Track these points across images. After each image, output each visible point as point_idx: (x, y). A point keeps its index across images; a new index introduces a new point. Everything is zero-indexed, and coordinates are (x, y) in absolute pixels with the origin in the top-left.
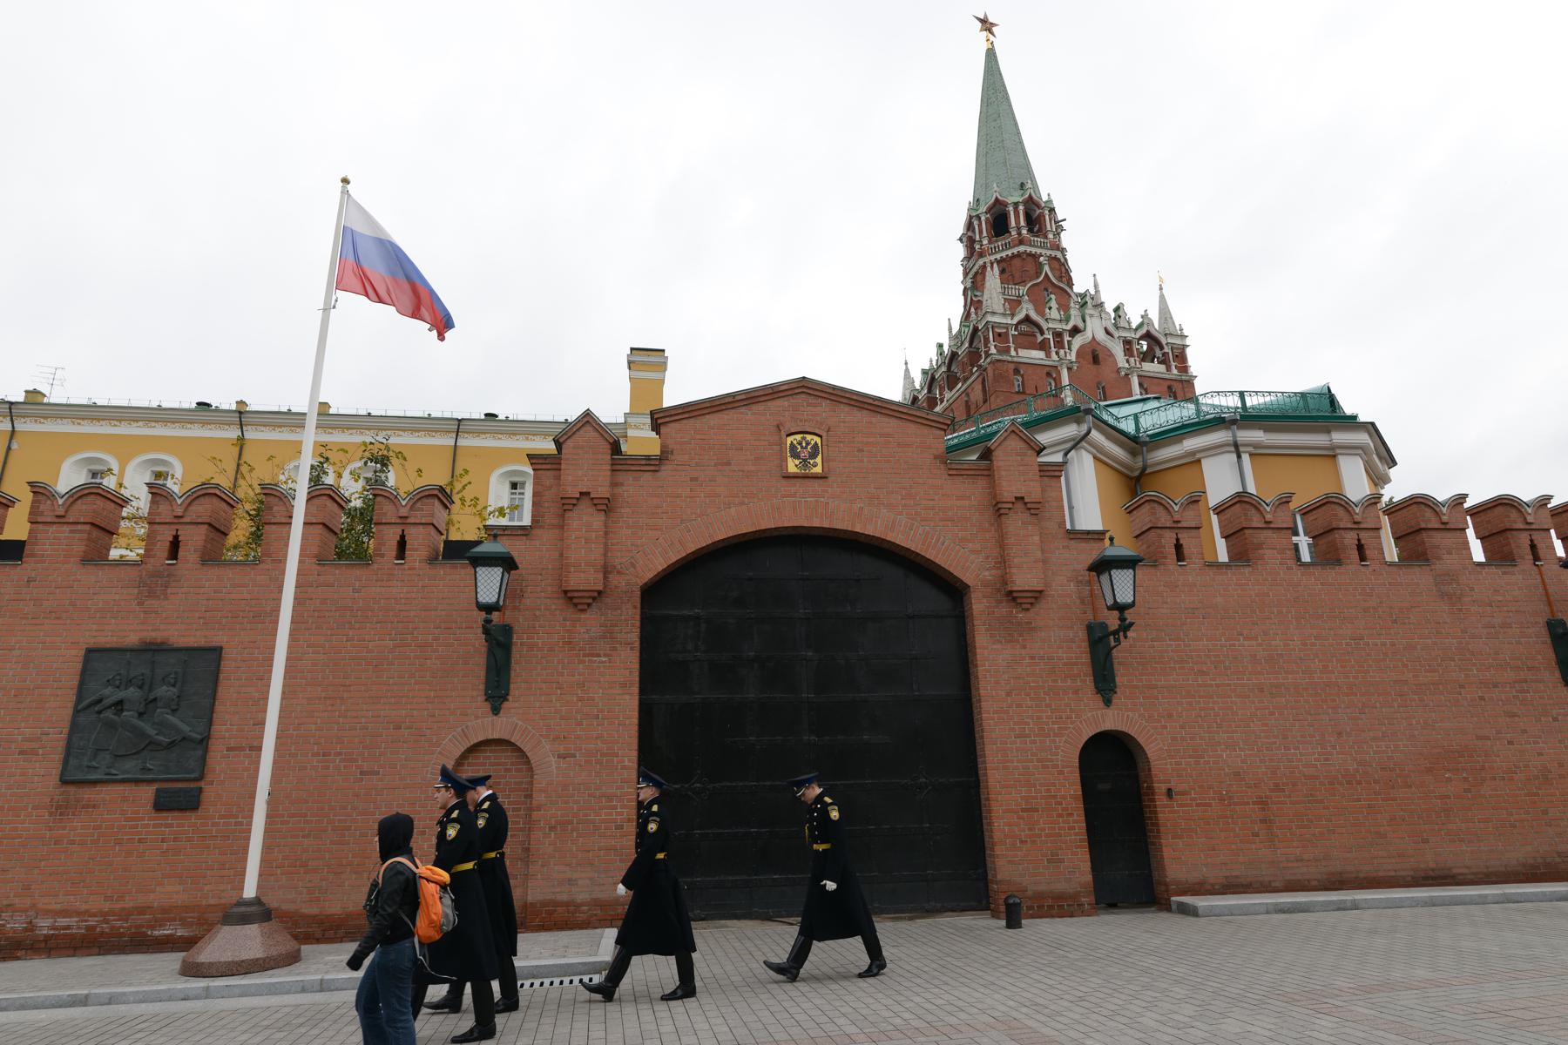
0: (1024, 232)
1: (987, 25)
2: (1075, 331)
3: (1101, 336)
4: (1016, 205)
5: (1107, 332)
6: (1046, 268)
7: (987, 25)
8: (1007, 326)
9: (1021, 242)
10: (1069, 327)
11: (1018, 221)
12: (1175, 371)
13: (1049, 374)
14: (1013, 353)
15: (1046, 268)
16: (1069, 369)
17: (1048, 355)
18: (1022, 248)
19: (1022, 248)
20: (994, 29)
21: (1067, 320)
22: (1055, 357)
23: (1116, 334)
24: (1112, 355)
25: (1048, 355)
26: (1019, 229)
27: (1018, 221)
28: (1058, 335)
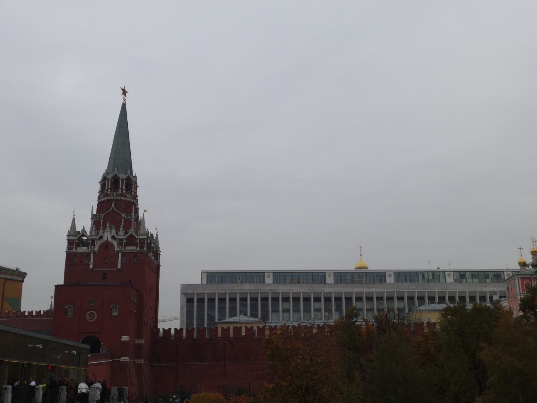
0: (109, 191)
1: (124, 92)
2: (101, 237)
3: (110, 239)
4: (108, 180)
5: (113, 237)
6: (113, 206)
7: (124, 92)
8: (74, 240)
9: (107, 195)
10: (98, 238)
11: (108, 187)
12: (138, 249)
13: (87, 256)
14: (74, 250)
15: (113, 206)
16: (94, 253)
17: (88, 249)
18: (106, 198)
19: (106, 198)
20: (127, 94)
21: (98, 234)
22: (90, 249)
23: (117, 237)
24: (113, 246)
25: (88, 249)
26: (107, 190)
27: (108, 187)
28: (93, 241)
